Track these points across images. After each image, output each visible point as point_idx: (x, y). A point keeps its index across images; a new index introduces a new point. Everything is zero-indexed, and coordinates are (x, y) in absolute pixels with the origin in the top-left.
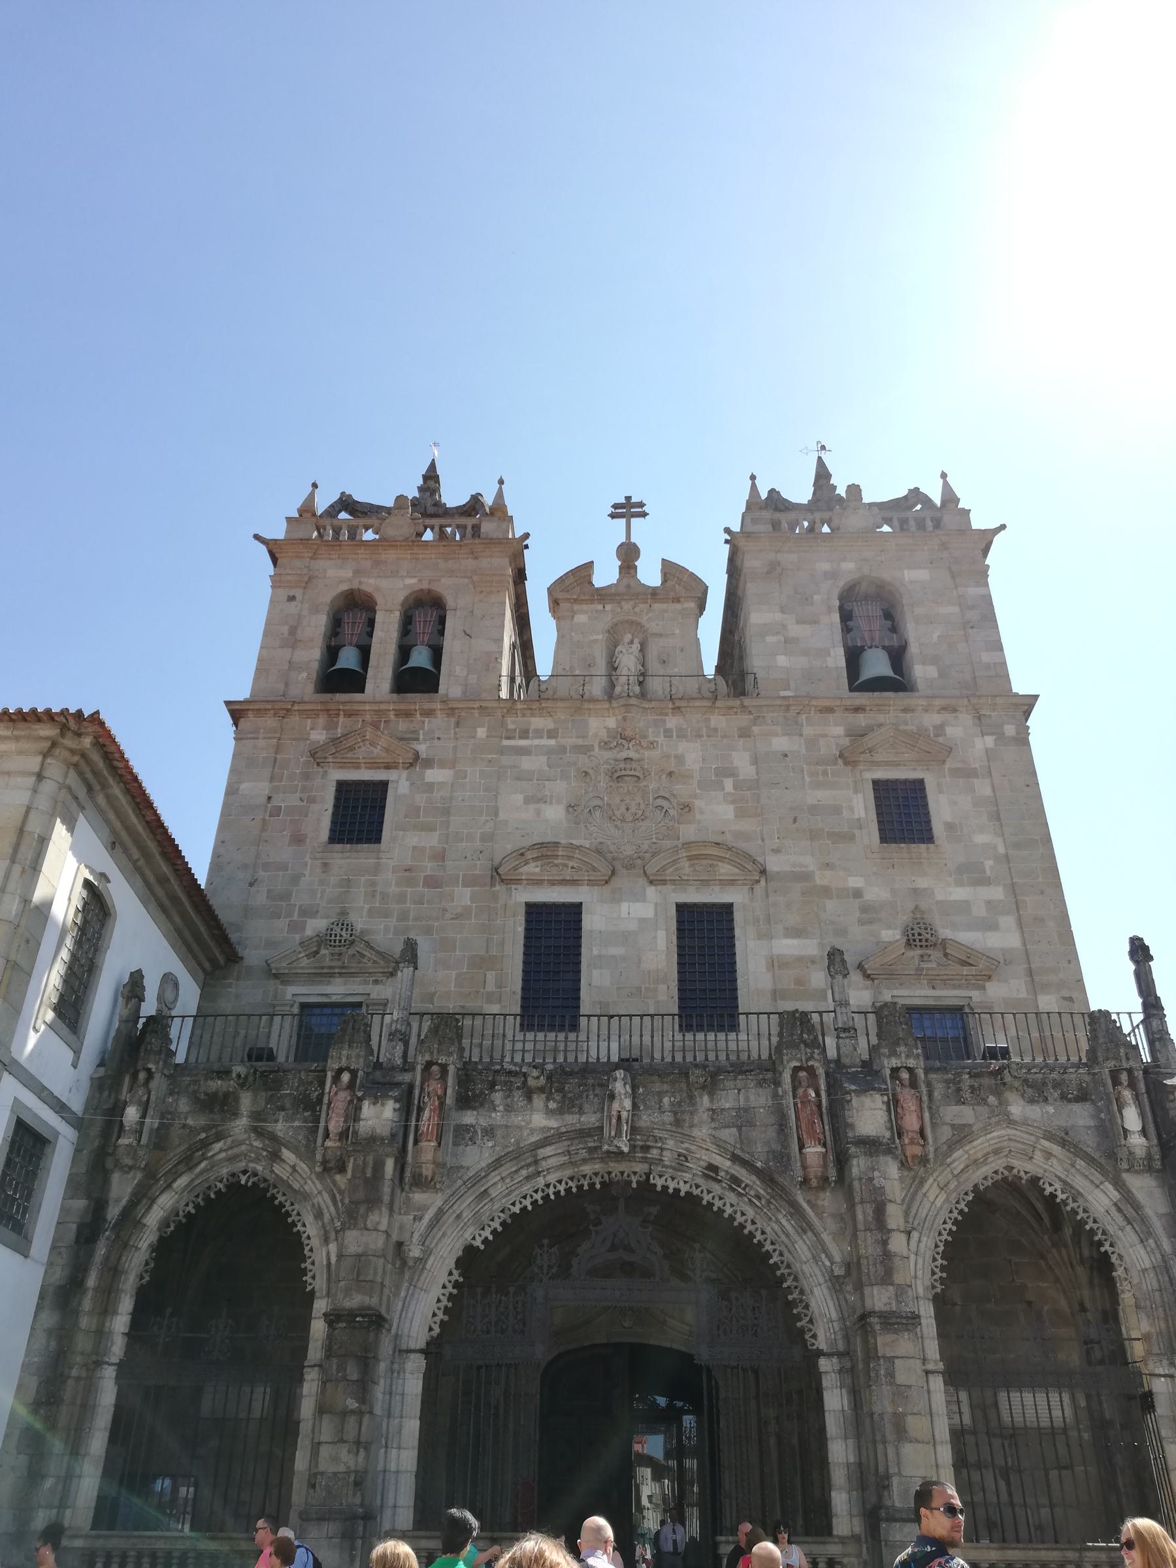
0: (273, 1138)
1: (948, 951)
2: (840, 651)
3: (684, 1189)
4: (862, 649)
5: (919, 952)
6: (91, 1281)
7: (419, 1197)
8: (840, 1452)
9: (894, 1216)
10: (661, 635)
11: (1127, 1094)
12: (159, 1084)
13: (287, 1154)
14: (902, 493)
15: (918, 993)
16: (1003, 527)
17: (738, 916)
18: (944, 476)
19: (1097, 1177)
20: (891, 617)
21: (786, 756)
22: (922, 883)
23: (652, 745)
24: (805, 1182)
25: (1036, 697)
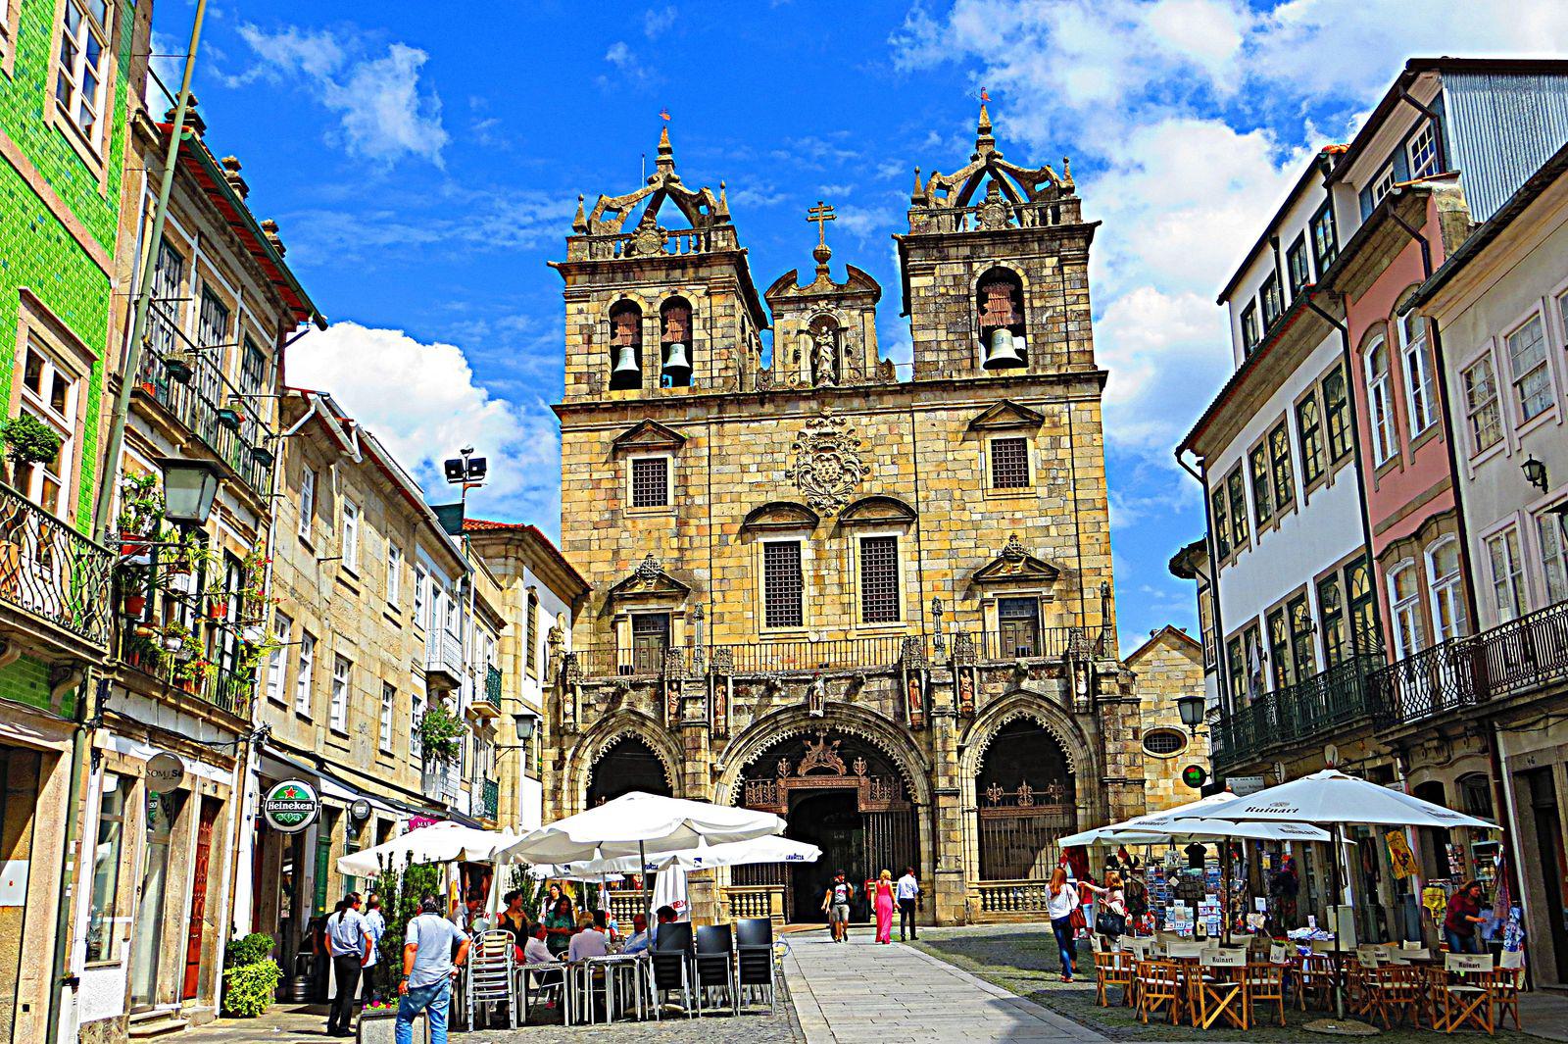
0: (640, 715)
2: (975, 336)
3: (853, 731)
6: (565, 786)
7: (718, 742)
8: (925, 847)
9: (953, 745)
10: (846, 329)
11: (1082, 674)
12: (579, 690)
13: (648, 723)
19: (1063, 716)
20: (1017, 297)
22: (1018, 515)
23: (842, 424)
24: (912, 728)
25: (1106, 372)
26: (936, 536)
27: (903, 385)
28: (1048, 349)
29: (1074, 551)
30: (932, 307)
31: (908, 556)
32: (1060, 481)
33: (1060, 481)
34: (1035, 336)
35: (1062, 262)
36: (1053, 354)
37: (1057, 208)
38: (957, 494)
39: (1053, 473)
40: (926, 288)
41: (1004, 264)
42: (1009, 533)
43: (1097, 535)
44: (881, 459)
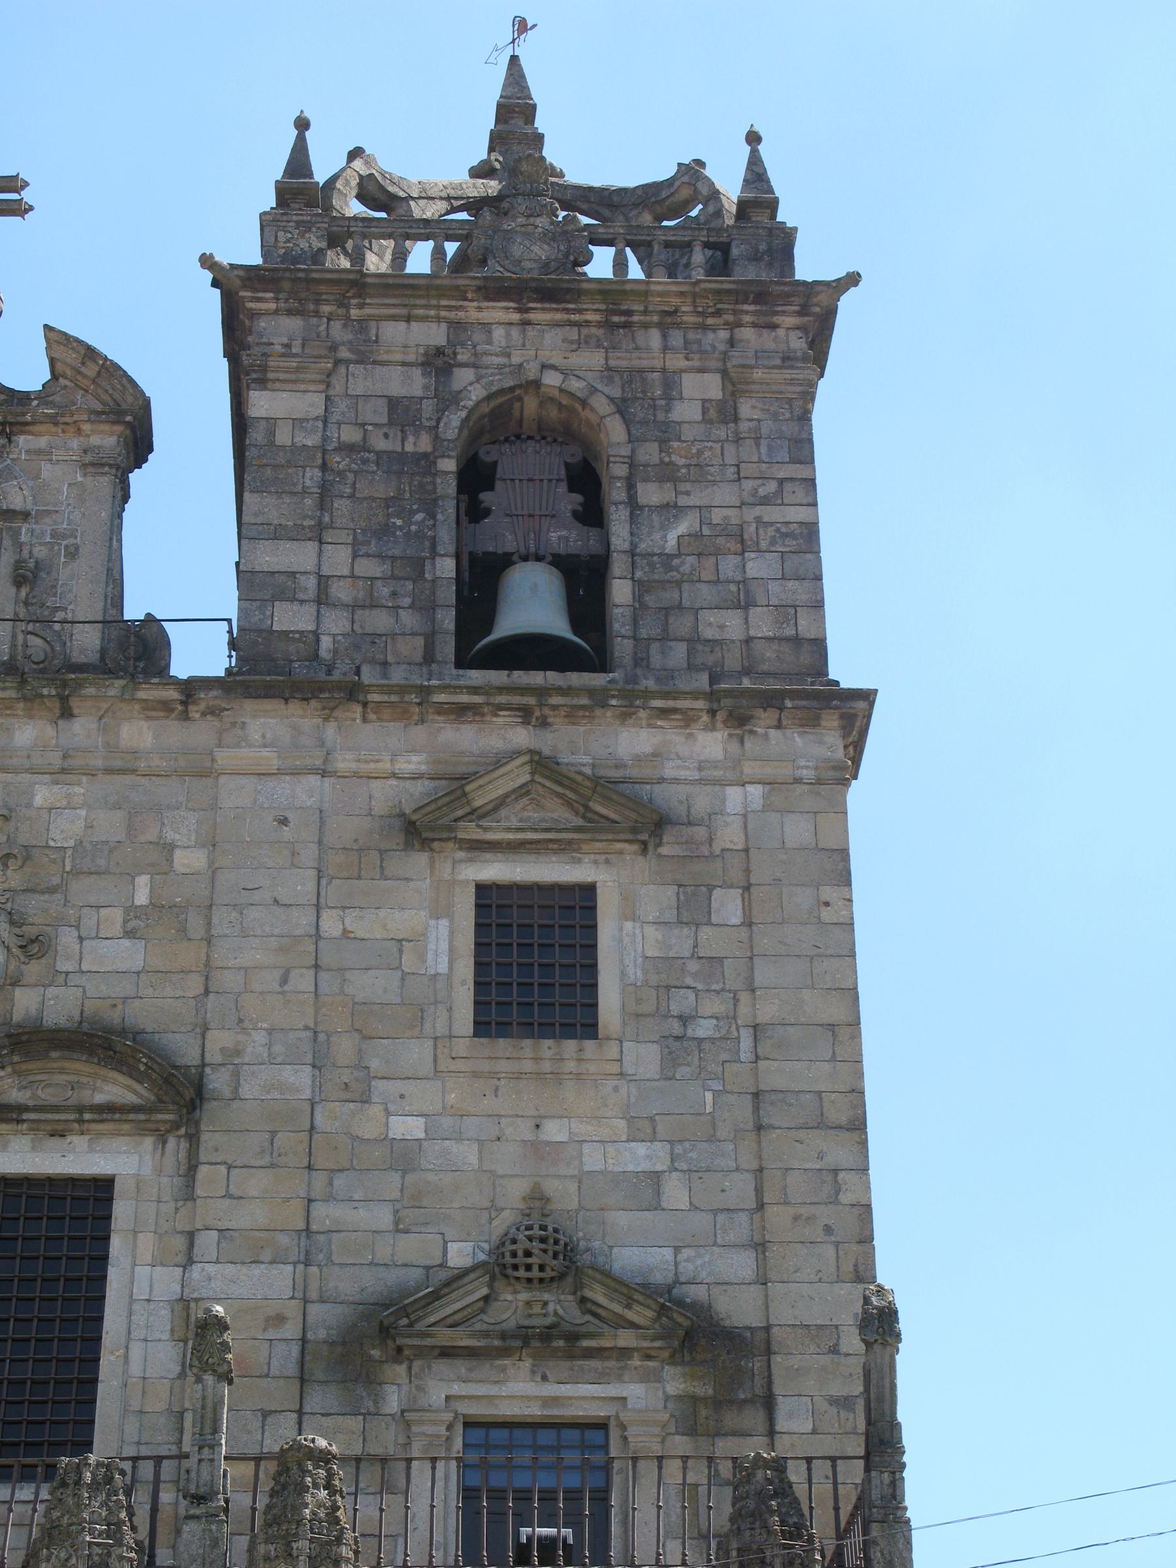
1: (588, 1294)
2: (447, 567)
4: (504, 562)
5: (524, 1296)
10: (26, 515)
14: (666, 172)
15: (505, 1390)
16: (853, 279)
17: (122, 1211)
18: (753, 138)
21: (284, 821)
22: (554, 1131)
25: (867, 697)
26: (255, 1183)
27: (192, 687)
28: (681, 625)
29: (742, 1265)
30: (312, 477)
31: (146, 1244)
32: (703, 1029)
33: (703, 1029)
34: (641, 588)
35: (735, 386)
36: (694, 640)
37: (725, 248)
38: (344, 1047)
39: (681, 1002)
40: (298, 423)
41: (551, 379)
42: (515, 1191)
43: (825, 1214)
44: (89, 919)
